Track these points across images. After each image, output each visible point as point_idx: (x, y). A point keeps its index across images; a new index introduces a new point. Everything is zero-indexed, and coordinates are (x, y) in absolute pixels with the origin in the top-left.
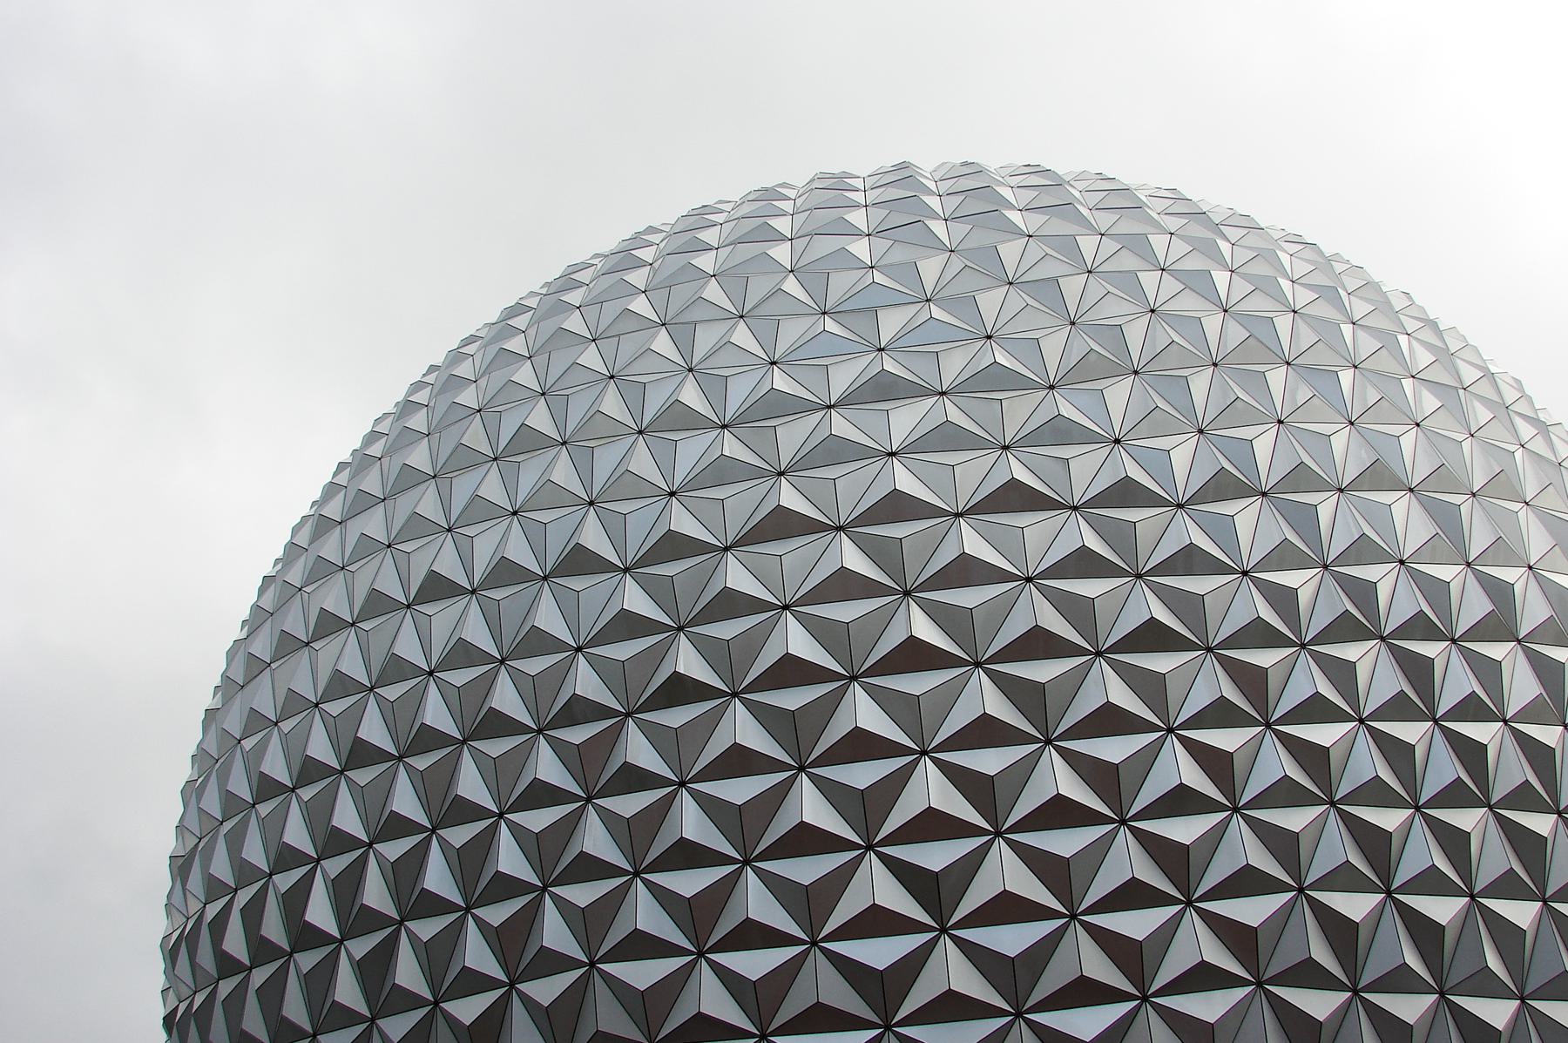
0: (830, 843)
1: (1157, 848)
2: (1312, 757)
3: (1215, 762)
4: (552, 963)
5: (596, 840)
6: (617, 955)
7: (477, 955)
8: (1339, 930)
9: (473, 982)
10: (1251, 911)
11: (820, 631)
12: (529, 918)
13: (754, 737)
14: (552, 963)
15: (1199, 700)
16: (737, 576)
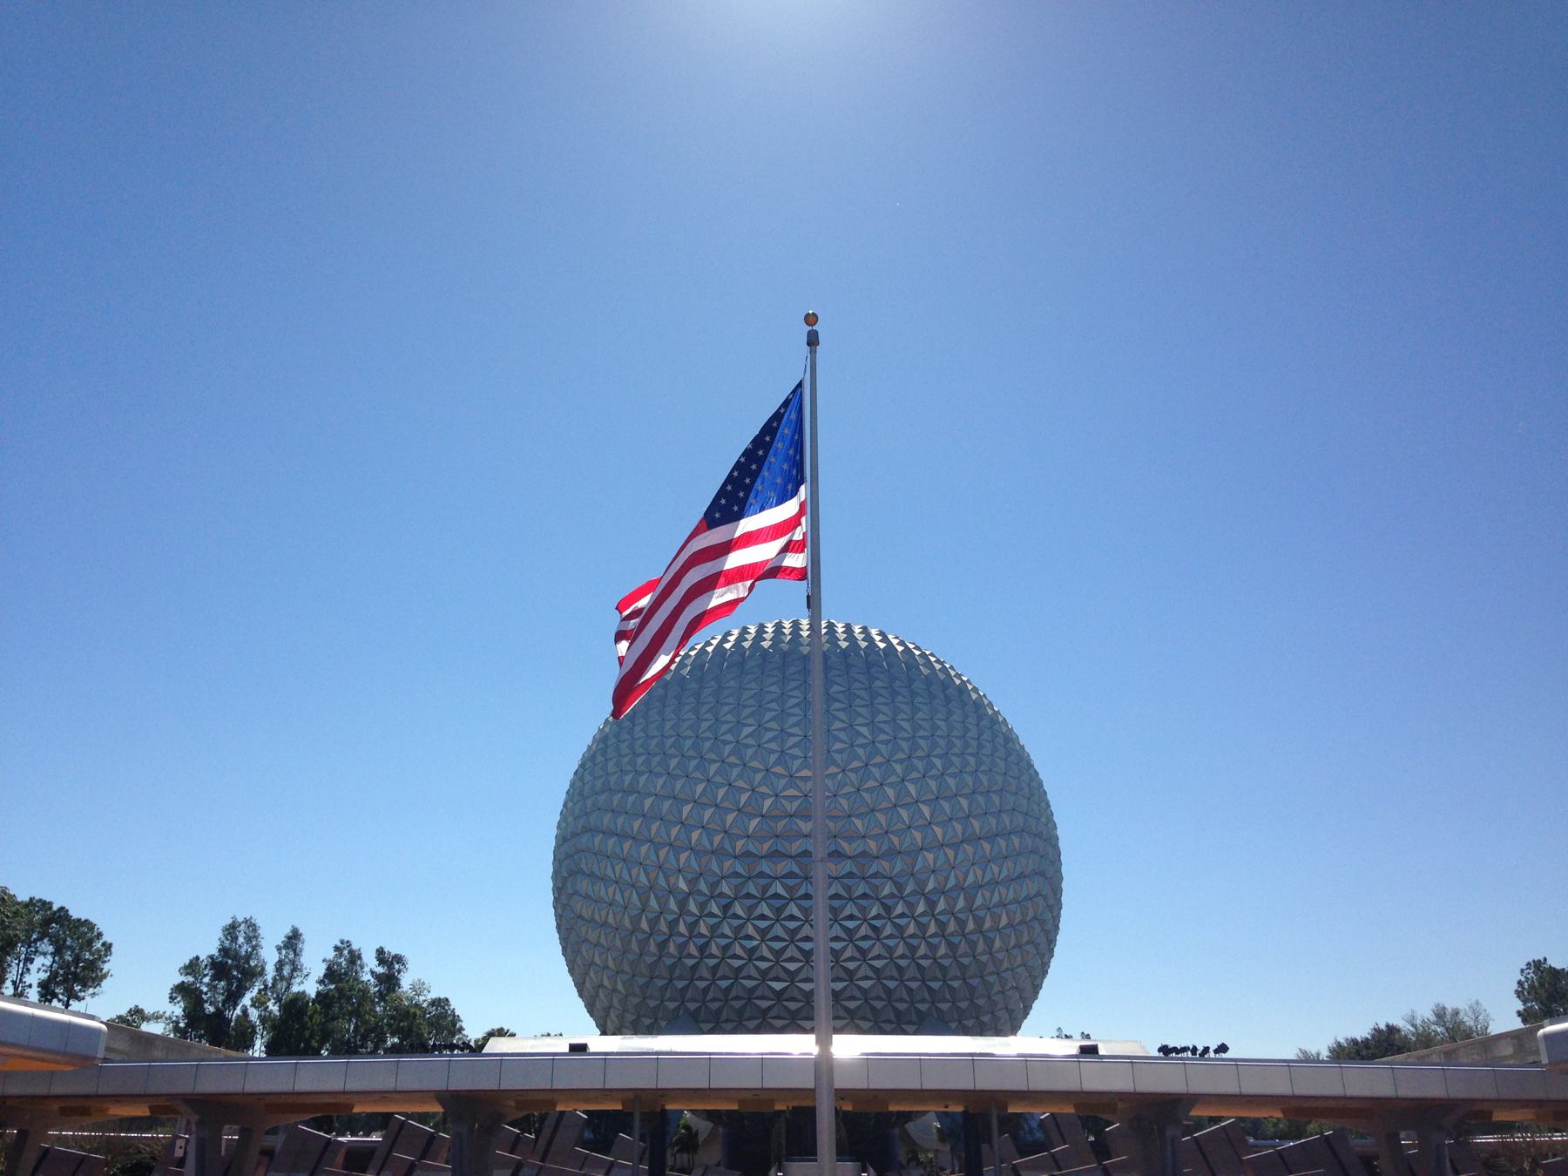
0: (783, 940)
1: (859, 949)
2: (901, 929)
3: (874, 928)
4: (712, 956)
5: (727, 931)
6: (729, 958)
7: (693, 950)
8: (900, 969)
9: (690, 956)
10: (878, 964)
11: (785, 886)
12: (707, 944)
13: (767, 912)
14: (712, 956)
15: (874, 912)
16: (765, 867)
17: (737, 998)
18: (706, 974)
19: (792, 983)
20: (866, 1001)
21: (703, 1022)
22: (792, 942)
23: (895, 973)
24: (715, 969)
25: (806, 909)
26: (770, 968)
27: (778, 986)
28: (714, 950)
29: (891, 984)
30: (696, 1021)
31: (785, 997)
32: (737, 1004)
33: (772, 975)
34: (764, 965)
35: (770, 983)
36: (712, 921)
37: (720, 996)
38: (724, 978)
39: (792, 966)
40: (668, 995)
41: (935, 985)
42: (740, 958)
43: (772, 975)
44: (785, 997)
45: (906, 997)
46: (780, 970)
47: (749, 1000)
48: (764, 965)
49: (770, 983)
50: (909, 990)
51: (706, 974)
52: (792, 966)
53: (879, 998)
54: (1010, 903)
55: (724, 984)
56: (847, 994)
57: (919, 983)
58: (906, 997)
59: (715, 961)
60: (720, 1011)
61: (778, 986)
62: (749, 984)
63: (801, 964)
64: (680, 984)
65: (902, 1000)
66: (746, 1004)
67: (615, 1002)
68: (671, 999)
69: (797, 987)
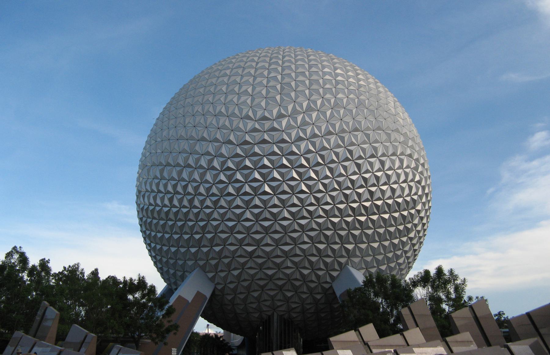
6: (219, 232)
17: (226, 257)
19: (258, 246)
20: (305, 256)
21: (209, 272)
22: (257, 221)
25: (265, 201)
26: (245, 238)
27: (250, 249)
28: (209, 228)
30: (205, 272)
32: (226, 261)
33: (246, 242)
34: (240, 236)
35: (244, 247)
36: (208, 211)
37: (216, 256)
38: (217, 245)
39: (258, 237)
40: (188, 257)
41: (350, 247)
43: (246, 242)
47: (233, 258)
48: (240, 236)
49: (244, 247)
52: (258, 237)
60: (217, 265)
61: (250, 249)
62: (232, 248)
63: (263, 235)
64: (193, 250)
66: (232, 260)
68: (190, 259)
69: (260, 248)
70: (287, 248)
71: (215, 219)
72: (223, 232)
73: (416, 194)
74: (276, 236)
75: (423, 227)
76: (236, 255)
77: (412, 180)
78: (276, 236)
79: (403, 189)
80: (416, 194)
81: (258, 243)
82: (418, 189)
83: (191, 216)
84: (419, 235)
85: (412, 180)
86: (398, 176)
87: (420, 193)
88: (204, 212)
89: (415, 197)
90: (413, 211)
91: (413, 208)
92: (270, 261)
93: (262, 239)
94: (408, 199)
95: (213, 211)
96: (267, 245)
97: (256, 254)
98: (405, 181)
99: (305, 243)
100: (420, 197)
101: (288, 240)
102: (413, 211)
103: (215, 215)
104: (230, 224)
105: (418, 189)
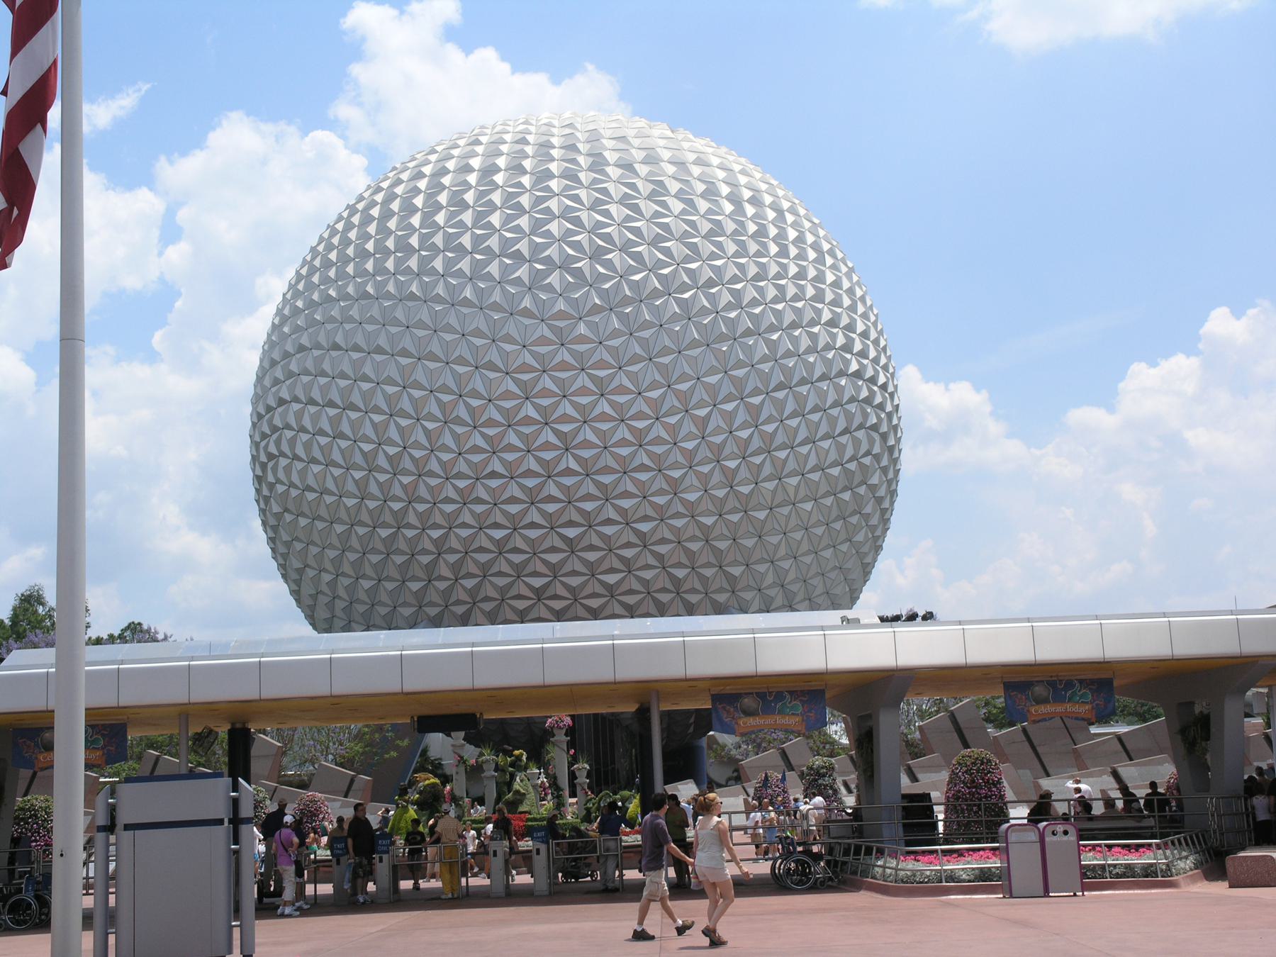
8: (691, 554)
17: (487, 599)
18: (445, 572)
23: (684, 560)
24: (456, 567)
29: (680, 573)
31: (548, 594)
33: (529, 569)
42: (488, 551)
44: (548, 594)
45: (698, 586)
46: (538, 563)
50: (704, 580)
51: (445, 572)
53: (664, 590)
54: (830, 466)
55: (469, 583)
56: (625, 587)
57: (715, 569)
58: (698, 586)
59: (458, 556)
65: (693, 591)
67: (339, 613)
70: (611, 579)
71: (464, 525)
72: (481, 550)
73: (868, 453)
74: (592, 556)
75: (892, 456)
76: (508, 596)
77: (860, 427)
78: (592, 556)
79: (841, 448)
80: (868, 453)
81: (554, 569)
82: (871, 442)
83: (412, 519)
84: (886, 477)
85: (860, 427)
86: (833, 421)
87: (877, 450)
88: (441, 511)
89: (867, 461)
90: (862, 490)
91: (863, 482)
92: (578, 605)
93: (564, 561)
94: (852, 466)
95: (460, 510)
96: (574, 573)
97: (549, 593)
98: (846, 431)
99: (648, 567)
100: (877, 458)
101: (617, 564)
102: (862, 490)
103: (467, 517)
104: (498, 534)
105: (871, 442)
